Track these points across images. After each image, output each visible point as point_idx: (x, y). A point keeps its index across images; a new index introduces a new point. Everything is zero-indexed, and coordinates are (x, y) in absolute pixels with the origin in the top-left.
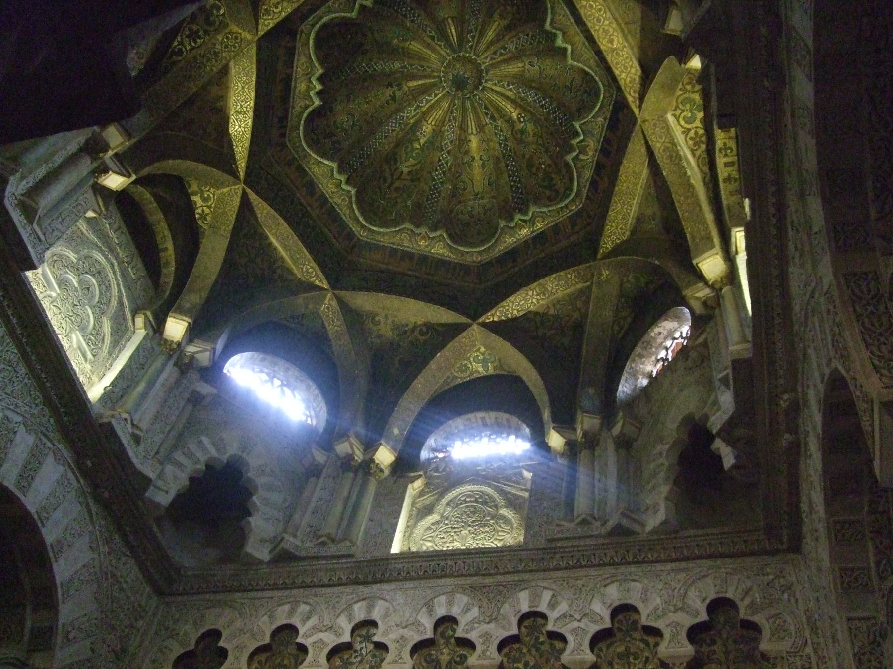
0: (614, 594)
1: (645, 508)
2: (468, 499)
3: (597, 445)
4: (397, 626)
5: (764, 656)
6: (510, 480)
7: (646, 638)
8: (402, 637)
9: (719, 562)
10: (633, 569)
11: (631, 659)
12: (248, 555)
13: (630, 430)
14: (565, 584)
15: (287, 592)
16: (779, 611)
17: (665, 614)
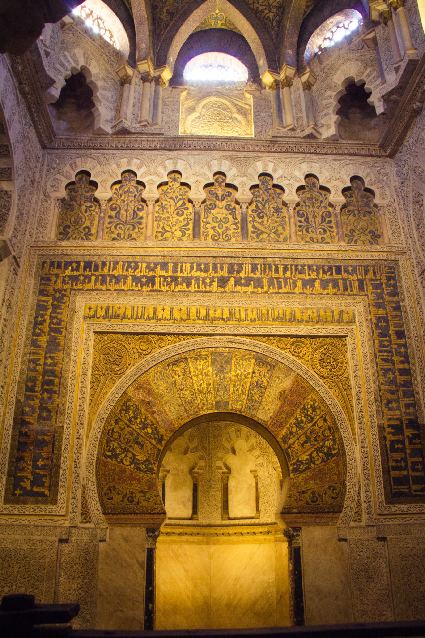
0: (306, 169)
1: (321, 125)
2: (214, 106)
3: (292, 85)
4: (193, 174)
5: (376, 206)
6: (237, 97)
7: (320, 191)
8: (197, 181)
9: (355, 158)
10: (313, 156)
11: (314, 200)
12: (100, 129)
13: (312, 81)
14: (280, 160)
15: (124, 152)
16: (381, 186)
17: (331, 181)
